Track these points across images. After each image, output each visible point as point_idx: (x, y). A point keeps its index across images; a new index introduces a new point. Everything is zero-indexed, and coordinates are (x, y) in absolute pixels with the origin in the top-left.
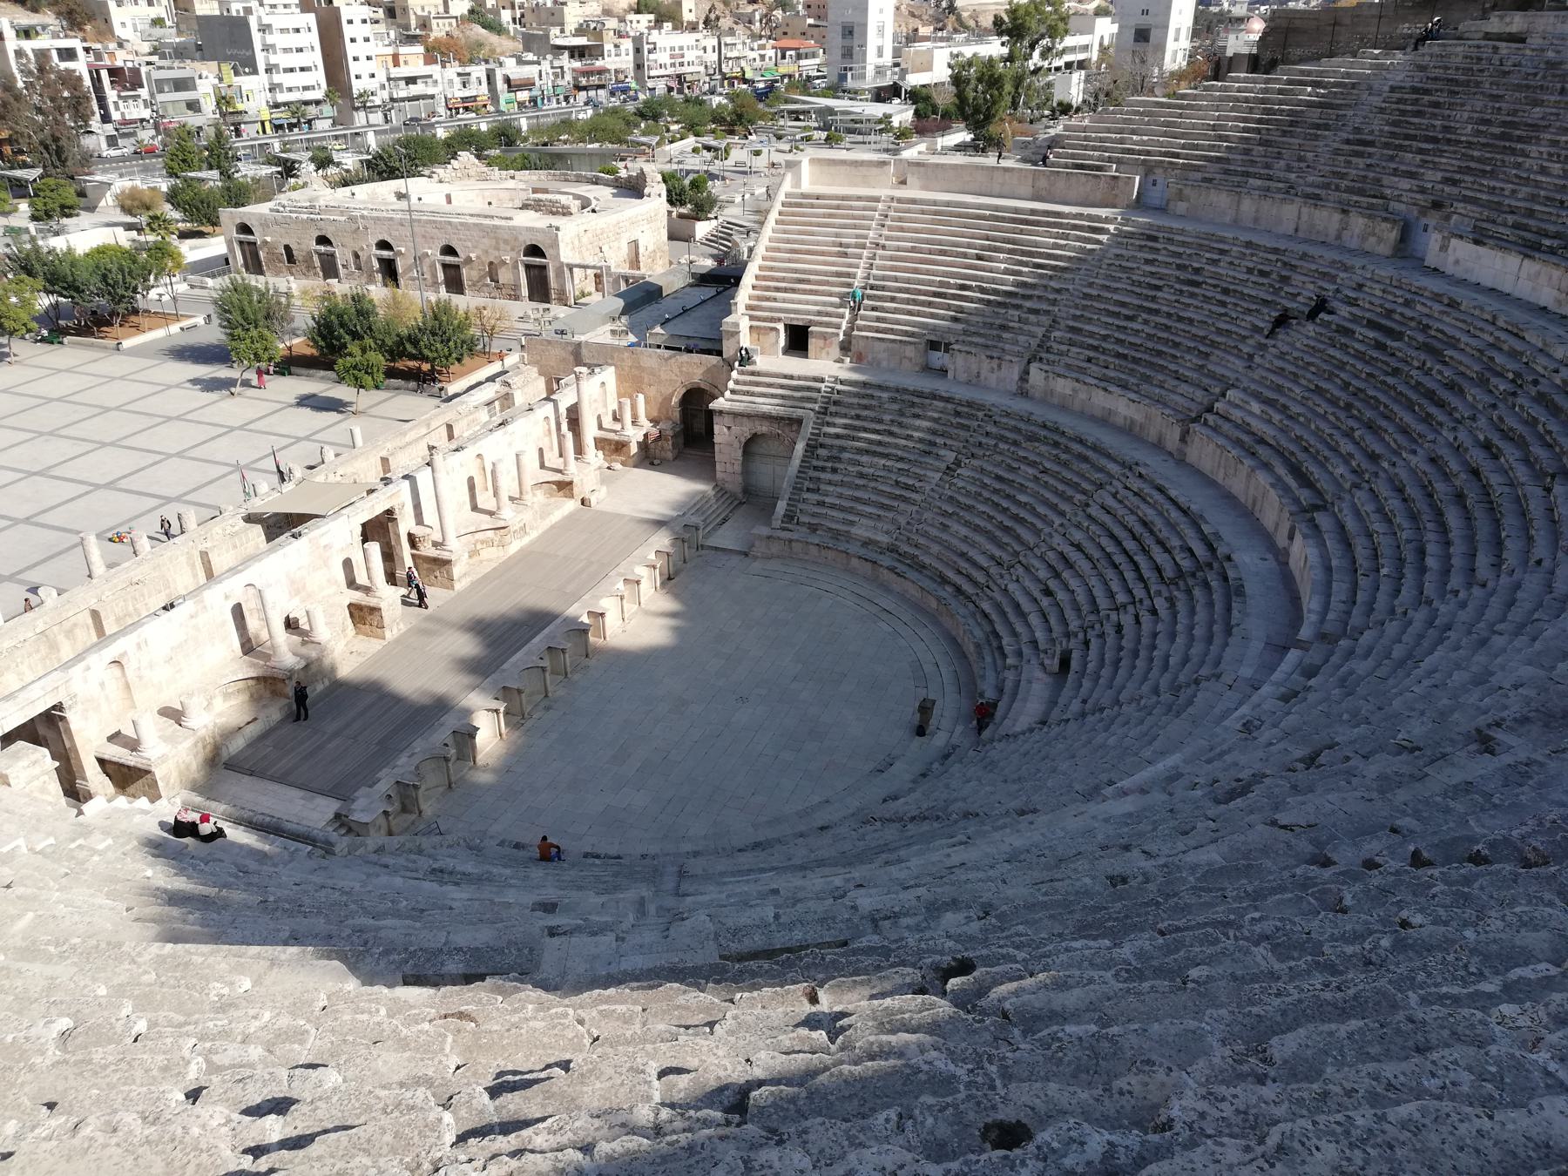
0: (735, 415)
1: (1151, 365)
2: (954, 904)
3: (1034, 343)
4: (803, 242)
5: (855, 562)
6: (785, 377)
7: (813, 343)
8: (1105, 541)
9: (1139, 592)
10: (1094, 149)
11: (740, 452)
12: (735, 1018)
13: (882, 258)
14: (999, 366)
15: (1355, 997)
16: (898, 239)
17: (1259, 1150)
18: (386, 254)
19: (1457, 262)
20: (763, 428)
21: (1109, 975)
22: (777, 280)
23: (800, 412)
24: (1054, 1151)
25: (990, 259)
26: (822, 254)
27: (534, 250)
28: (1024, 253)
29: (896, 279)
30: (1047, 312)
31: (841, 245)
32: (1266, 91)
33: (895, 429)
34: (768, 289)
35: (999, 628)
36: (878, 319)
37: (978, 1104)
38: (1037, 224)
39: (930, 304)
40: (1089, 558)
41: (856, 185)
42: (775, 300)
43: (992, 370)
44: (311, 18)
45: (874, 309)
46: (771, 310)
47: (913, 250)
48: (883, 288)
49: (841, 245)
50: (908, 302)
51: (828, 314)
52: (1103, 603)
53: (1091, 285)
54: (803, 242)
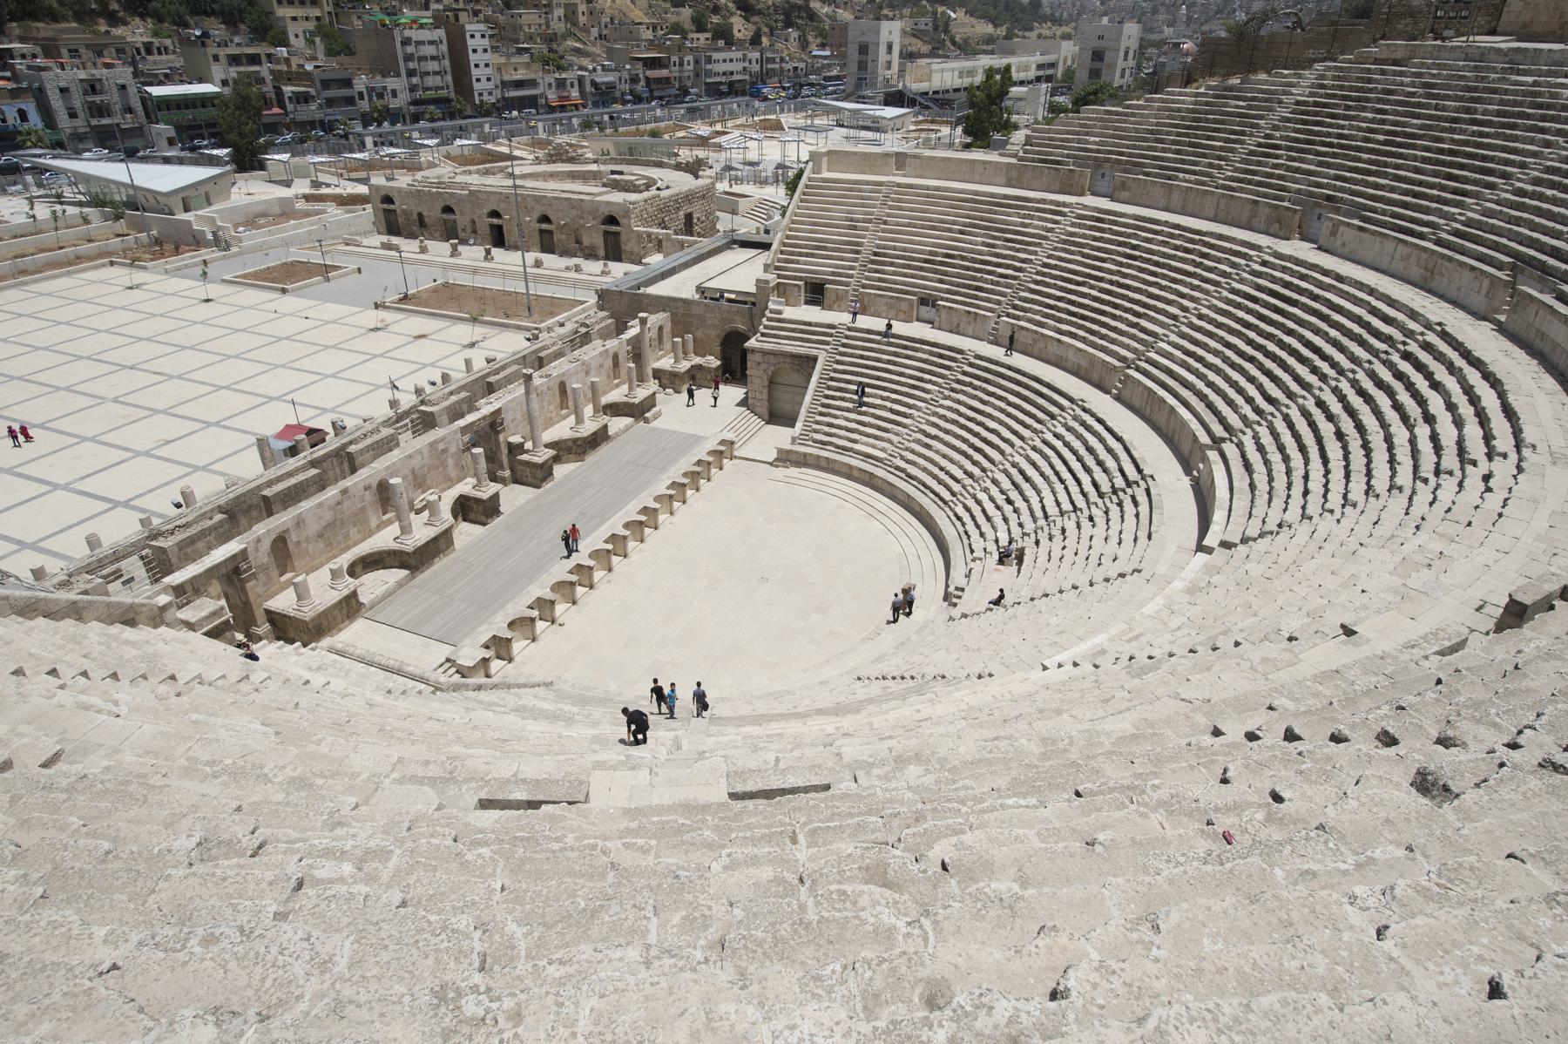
0: (765, 353)
2: (917, 757)
4: (821, 217)
6: (805, 323)
7: (829, 297)
9: (1080, 502)
10: (1057, 147)
12: (729, 855)
15: (1231, 871)
17: (1139, 1032)
18: (495, 221)
19: (1344, 245)
21: (1031, 833)
23: (814, 352)
24: (967, 1014)
27: (611, 220)
28: (997, 230)
29: (895, 249)
30: (1015, 278)
32: (1196, 103)
34: (792, 254)
36: (880, 280)
37: (910, 960)
38: (1009, 206)
39: (921, 269)
44: (441, 33)
50: (904, 266)
51: (840, 275)
52: (1052, 510)
54: (821, 217)
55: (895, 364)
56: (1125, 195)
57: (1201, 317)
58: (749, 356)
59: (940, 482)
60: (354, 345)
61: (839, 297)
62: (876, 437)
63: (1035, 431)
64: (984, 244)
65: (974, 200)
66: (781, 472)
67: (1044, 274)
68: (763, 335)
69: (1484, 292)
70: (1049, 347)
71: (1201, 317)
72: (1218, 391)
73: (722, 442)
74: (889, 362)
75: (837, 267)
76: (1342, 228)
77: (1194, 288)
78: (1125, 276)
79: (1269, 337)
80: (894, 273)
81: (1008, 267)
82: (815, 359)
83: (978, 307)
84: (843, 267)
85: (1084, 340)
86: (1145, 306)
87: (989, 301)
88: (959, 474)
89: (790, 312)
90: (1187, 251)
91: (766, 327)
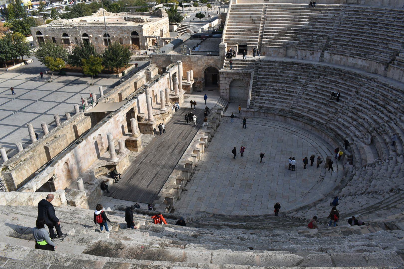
0: (227, 73)
1: (367, 48)
3: (324, 45)
4: (240, 20)
5: (277, 117)
8: (370, 102)
11: (228, 87)
13: (267, 23)
16: (271, 17)
18: (86, 37)
20: (237, 77)
22: (233, 31)
23: (249, 71)
25: (303, 21)
26: (247, 23)
27: (134, 33)
29: (273, 29)
30: (326, 36)
31: (252, 20)
33: (282, 74)
34: (231, 34)
35: (339, 132)
39: (285, 36)
40: (366, 108)
41: (252, 2)
42: (234, 37)
43: (311, 54)
45: (267, 38)
46: (233, 41)
47: (276, 20)
48: (269, 32)
50: (278, 35)
51: (252, 41)
53: (339, 27)
54: (240, 20)
58: (221, 76)
60: (42, 88)
62: (283, 102)
75: (250, 38)
80: (274, 39)
84: (253, 38)
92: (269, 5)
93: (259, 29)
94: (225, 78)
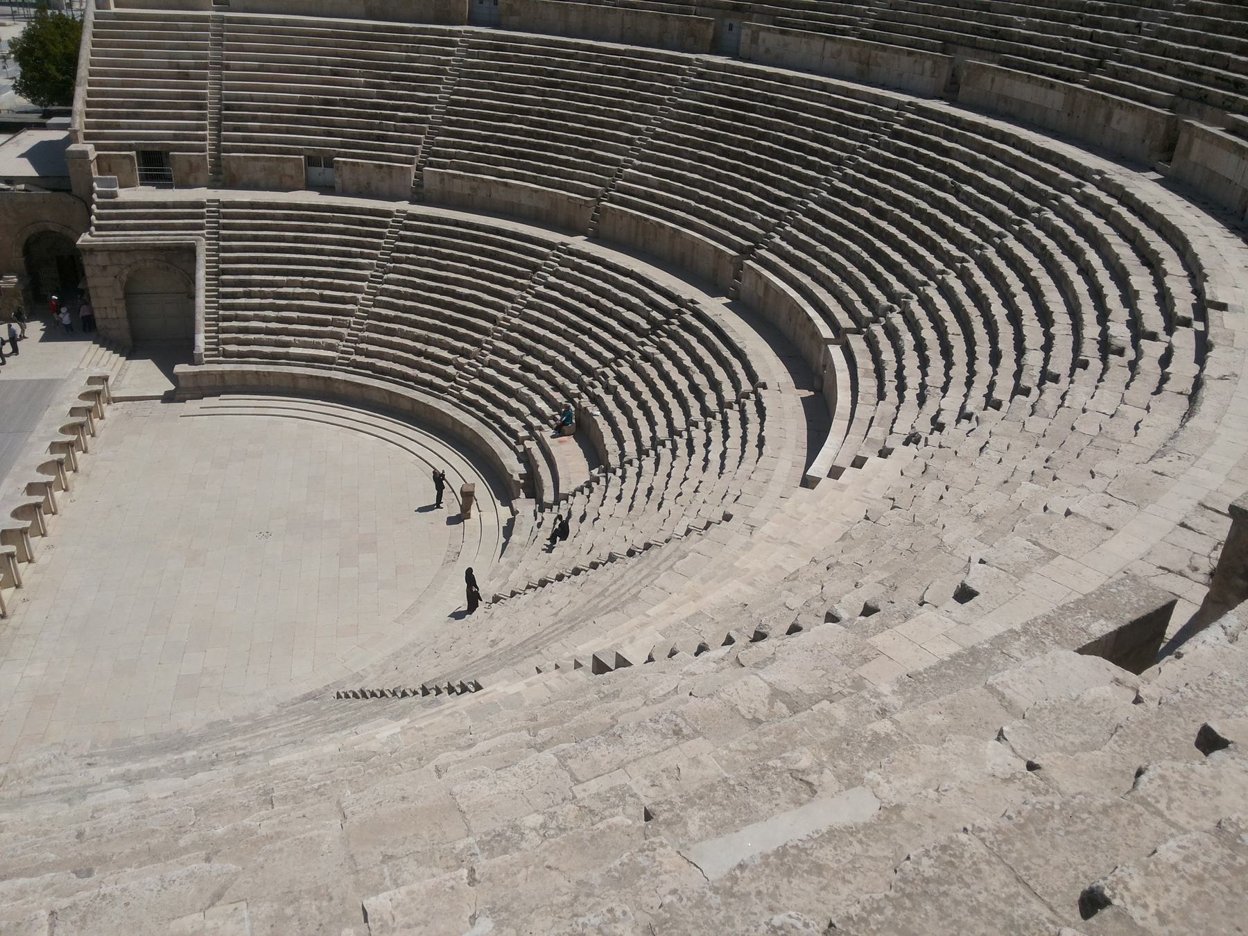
0: (111, 251)
13: (229, 78)
14: (390, 174)
19: (767, 50)
26: (160, 76)
28: (379, 67)
29: (252, 99)
31: (178, 66)
39: (297, 121)
48: (240, 108)
49: (178, 66)
50: (272, 120)
55: (305, 240)
56: (514, 19)
57: (657, 136)
58: (86, 260)
59: (423, 369)
61: (194, 167)
63: (521, 288)
64: (367, 85)
65: (339, 34)
66: (192, 406)
67: (456, 113)
68: (99, 228)
69: (928, 73)
70: (494, 195)
71: (657, 136)
72: (716, 205)
73: (91, 380)
74: (296, 240)
75: (178, 127)
76: (762, 35)
77: (634, 108)
78: (554, 105)
79: (741, 144)
80: (262, 130)
81: (409, 109)
82: (191, 250)
83: (389, 159)
84: (187, 128)
85: (535, 180)
86: (590, 134)
87: (400, 151)
88: (445, 354)
89: (124, 195)
90: (611, 72)
91: (99, 217)
92: (230, 20)
93: (204, 97)
94: (105, 267)
